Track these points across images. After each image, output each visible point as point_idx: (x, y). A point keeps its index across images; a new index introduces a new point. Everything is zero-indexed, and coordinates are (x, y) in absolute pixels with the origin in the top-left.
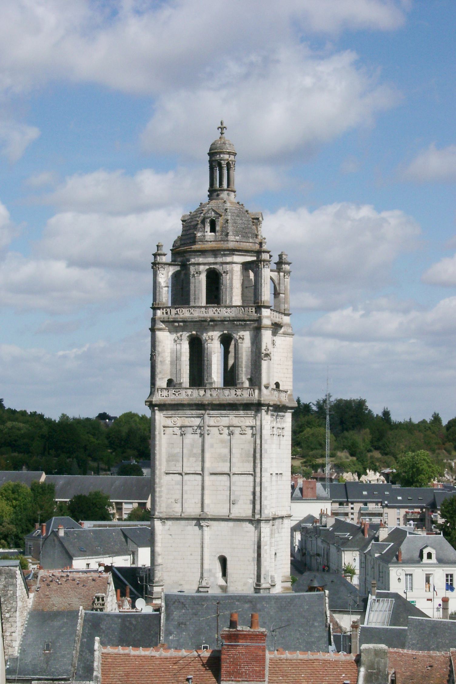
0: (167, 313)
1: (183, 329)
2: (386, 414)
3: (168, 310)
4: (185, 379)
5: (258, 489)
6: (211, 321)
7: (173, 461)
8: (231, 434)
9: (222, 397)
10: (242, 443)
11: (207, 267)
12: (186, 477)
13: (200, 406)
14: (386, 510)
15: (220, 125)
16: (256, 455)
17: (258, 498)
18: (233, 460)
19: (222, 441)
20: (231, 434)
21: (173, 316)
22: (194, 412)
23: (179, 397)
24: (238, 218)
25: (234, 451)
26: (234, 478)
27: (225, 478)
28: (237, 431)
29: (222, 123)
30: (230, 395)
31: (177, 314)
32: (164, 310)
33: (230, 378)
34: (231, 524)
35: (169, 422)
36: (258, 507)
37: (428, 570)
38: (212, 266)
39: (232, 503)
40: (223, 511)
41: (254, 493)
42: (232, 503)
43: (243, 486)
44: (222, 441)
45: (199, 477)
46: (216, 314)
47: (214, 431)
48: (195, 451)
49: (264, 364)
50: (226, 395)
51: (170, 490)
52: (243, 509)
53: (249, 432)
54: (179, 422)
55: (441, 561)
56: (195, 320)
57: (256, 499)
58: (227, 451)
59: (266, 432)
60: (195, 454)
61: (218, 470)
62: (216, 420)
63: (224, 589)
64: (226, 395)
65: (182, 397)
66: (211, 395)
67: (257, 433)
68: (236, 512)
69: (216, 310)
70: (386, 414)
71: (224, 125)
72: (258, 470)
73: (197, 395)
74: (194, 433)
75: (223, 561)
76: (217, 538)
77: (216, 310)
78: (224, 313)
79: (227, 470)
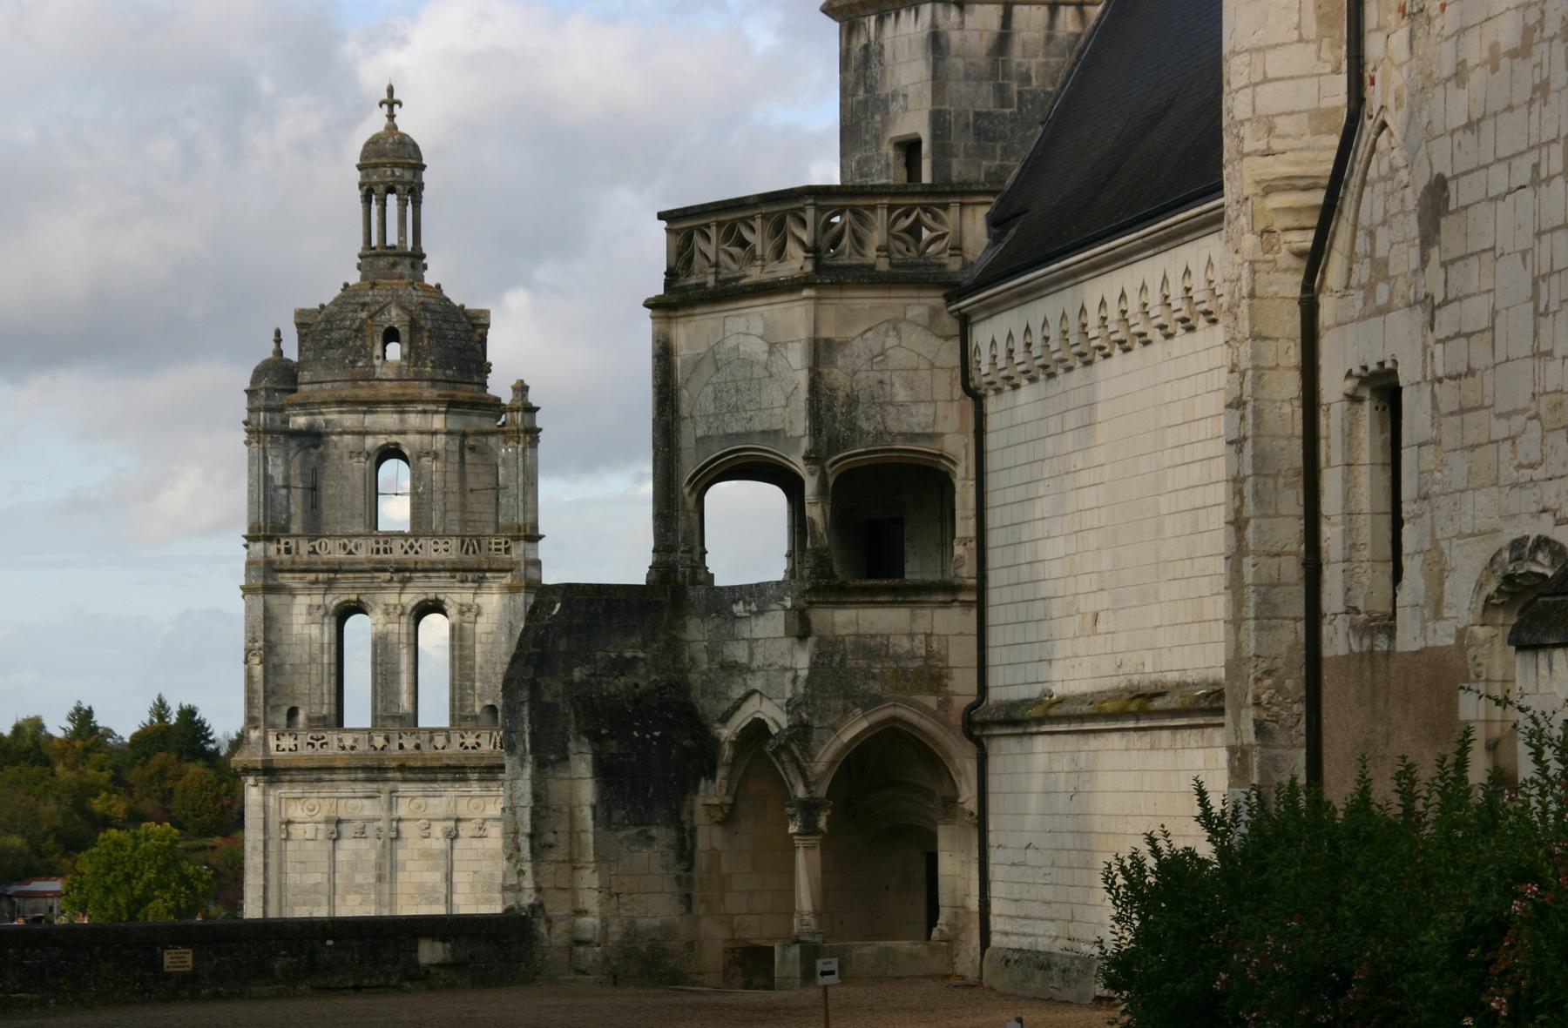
0: (288, 551)
3: (292, 542)
6: (397, 571)
7: (304, 904)
8: (452, 836)
11: (381, 440)
15: (385, 97)
19: (426, 854)
20: (452, 836)
21: (305, 557)
22: (359, 787)
23: (321, 752)
24: (445, 326)
25: (456, 877)
28: (466, 829)
29: (391, 90)
31: (314, 552)
32: (283, 541)
38: (395, 439)
46: (411, 553)
48: (359, 879)
50: (440, 746)
54: (325, 809)
56: (359, 567)
60: (361, 886)
64: (440, 746)
65: (330, 752)
66: (401, 746)
69: (411, 547)
71: (396, 97)
74: (361, 834)
77: (411, 547)
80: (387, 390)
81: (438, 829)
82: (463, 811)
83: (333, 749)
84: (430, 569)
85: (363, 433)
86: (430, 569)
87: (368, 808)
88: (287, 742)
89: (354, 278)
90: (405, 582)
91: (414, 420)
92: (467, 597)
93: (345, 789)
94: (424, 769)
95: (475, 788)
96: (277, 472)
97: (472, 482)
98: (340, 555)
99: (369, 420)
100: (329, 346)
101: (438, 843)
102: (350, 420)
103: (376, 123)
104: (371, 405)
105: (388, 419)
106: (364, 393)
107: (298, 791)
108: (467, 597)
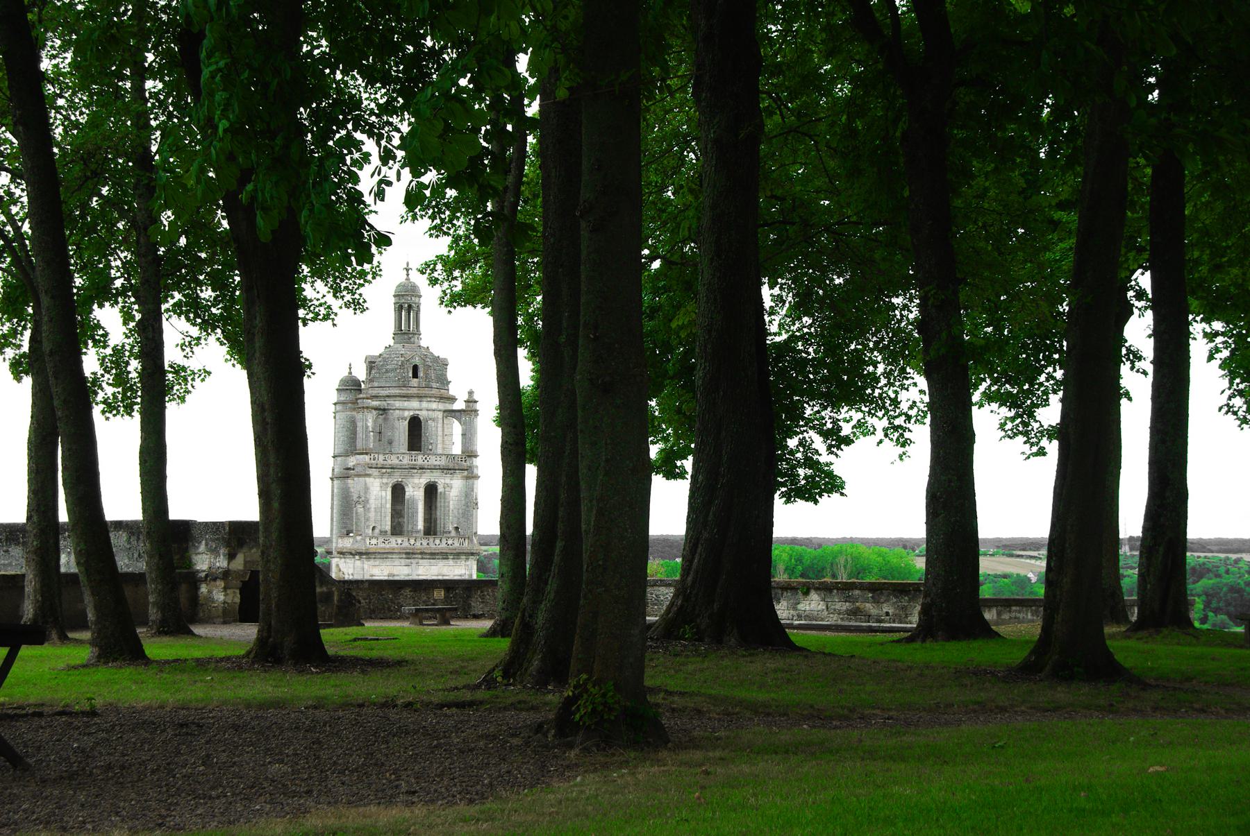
1: (390, 475)
4: (388, 528)
11: (412, 413)
22: (403, 561)
73: (395, 542)
78: (433, 461)
80: (414, 391)
83: (393, 545)
84: (433, 468)
86: (433, 468)
88: (374, 541)
89: (392, 342)
91: (425, 405)
92: (448, 481)
93: (397, 562)
94: (432, 554)
95: (451, 562)
99: (406, 404)
100: (387, 371)
102: (398, 404)
104: (407, 397)
105: (414, 404)
106: (404, 391)
107: (377, 562)
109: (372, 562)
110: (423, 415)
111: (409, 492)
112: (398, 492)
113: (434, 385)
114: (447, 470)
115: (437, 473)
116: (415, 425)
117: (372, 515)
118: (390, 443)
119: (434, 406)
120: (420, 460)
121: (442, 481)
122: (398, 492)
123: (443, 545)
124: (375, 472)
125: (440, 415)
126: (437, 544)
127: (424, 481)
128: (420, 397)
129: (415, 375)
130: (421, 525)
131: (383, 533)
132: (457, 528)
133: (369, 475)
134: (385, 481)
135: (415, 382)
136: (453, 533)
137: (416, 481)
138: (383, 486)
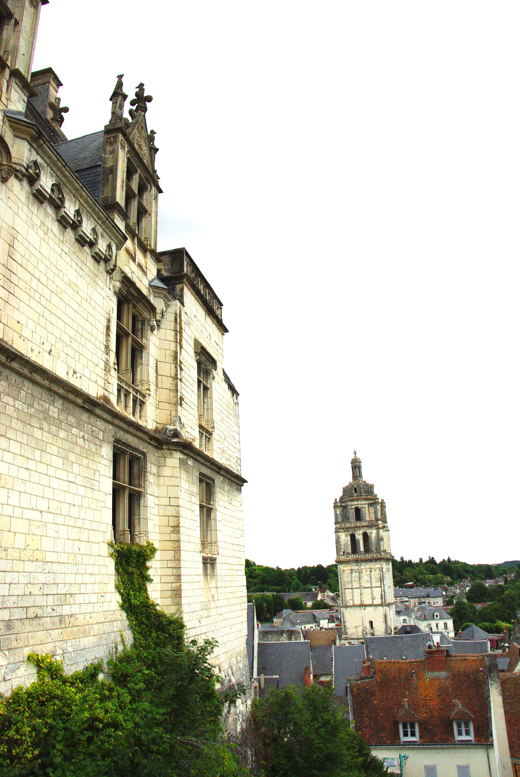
1: (348, 531)
2: (402, 558)
4: (350, 551)
5: (383, 593)
8: (371, 571)
9: (365, 557)
10: (376, 574)
12: (354, 590)
13: (357, 561)
14: (410, 599)
16: (382, 579)
17: (383, 596)
18: (373, 582)
20: (371, 571)
25: (372, 578)
26: (374, 589)
27: (369, 589)
28: (373, 570)
30: (369, 556)
33: (367, 550)
34: (373, 608)
35: (345, 568)
36: (384, 600)
37: (437, 622)
39: (373, 599)
40: (370, 603)
41: (382, 595)
42: (373, 599)
43: (377, 592)
44: (367, 575)
45: (380, 589)
47: (364, 571)
49: (381, 542)
51: (350, 596)
52: (378, 601)
53: (378, 570)
55: (441, 618)
57: (383, 597)
58: (369, 578)
59: (384, 570)
61: (367, 586)
62: (365, 567)
63: (373, 634)
67: (381, 570)
68: (375, 602)
70: (402, 558)
72: (382, 585)
74: (356, 572)
75: (371, 623)
76: (370, 613)
78: (363, 524)
79: (370, 586)
80: (356, 498)
81: (368, 570)
82: (372, 566)
83: (350, 558)
84: (364, 527)
85: (352, 505)
86: (364, 527)
87: (357, 567)
88: (343, 557)
89: (351, 481)
90: (360, 529)
91: (359, 502)
92: (370, 531)
93: (353, 565)
95: (374, 563)
96: (338, 512)
97: (371, 512)
98: (349, 525)
101: (369, 573)
102: (349, 503)
103: (353, 456)
104: (353, 500)
105: (356, 503)
108: (370, 531)
109: (343, 565)
110: (359, 506)
111: (357, 537)
112: (353, 537)
113: (364, 494)
114: (370, 526)
115: (366, 528)
116: (358, 511)
117: (342, 547)
118: (348, 518)
119: (363, 502)
120: (358, 524)
121: (368, 531)
122: (353, 537)
123: (370, 556)
124: (342, 530)
125: (367, 506)
126: (369, 556)
127: (361, 532)
128: (357, 500)
129: (356, 492)
130: (362, 549)
131: (348, 553)
132: (376, 549)
133: (339, 532)
134: (346, 533)
135: (355, 494)
136: (375, 551)
137: (358, 532)
138: (346, 535)
